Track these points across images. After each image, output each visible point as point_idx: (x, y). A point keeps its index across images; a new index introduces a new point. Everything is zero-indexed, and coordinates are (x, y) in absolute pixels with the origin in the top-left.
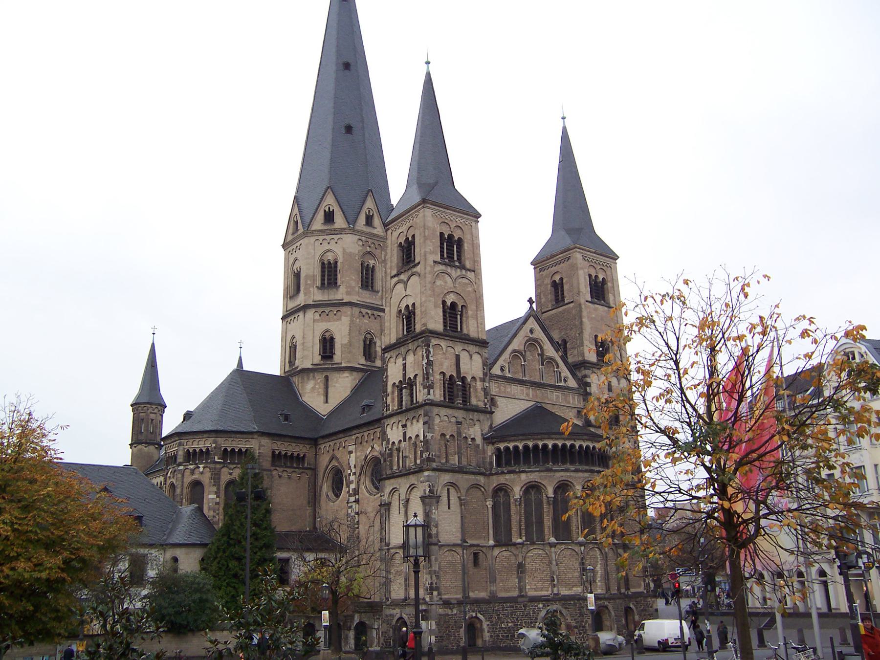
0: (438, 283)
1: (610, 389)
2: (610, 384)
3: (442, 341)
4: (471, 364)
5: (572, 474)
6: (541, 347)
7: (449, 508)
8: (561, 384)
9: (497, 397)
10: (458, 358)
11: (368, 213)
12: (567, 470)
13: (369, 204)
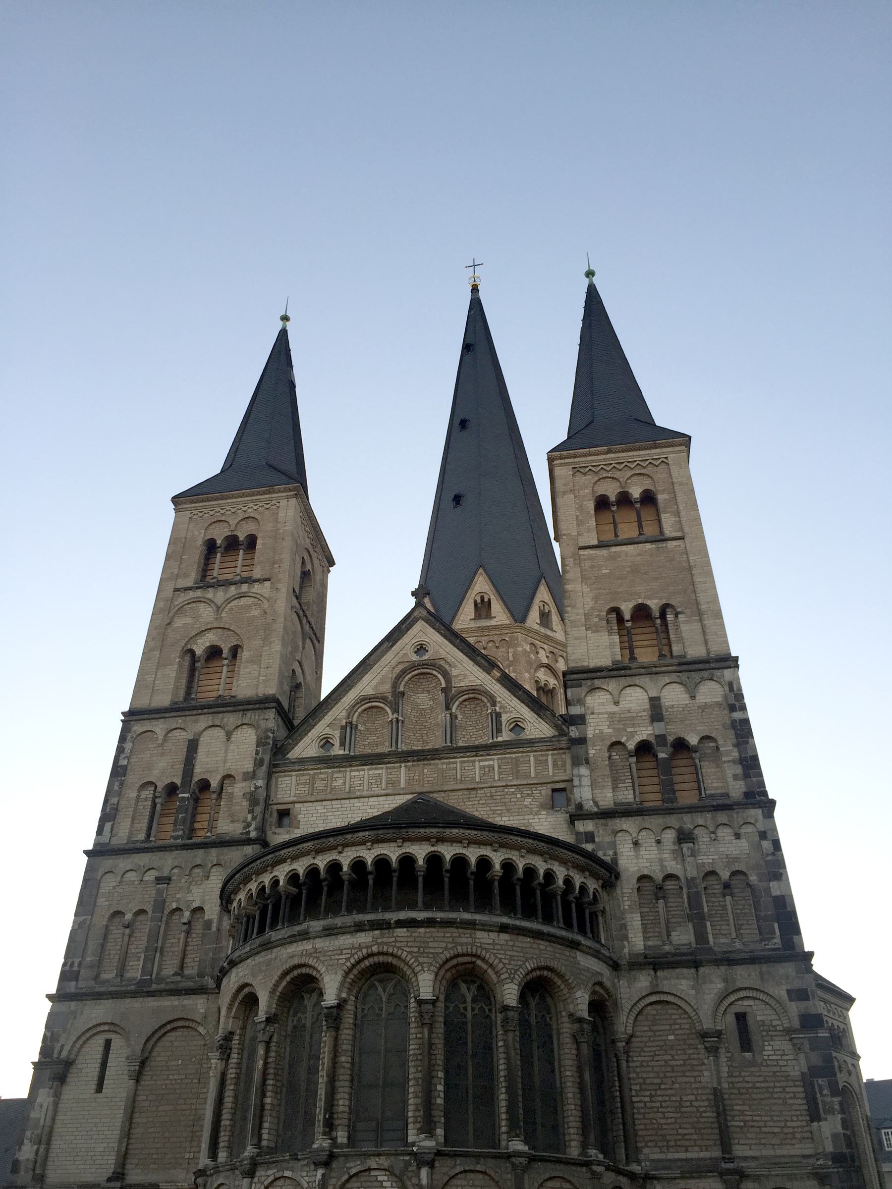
0: (179, 623)
1: (656, 711)
2: (655, 703)
3: (155, 722)
4: (226, 751)
5: (320, 944)
6: (446, 674)
7: (100, 1088)
8: (500, 739)
9: (297, 805)
10: (193, 746)
11: (542, 608)
12: (305, 936)
13: (543, 594)
